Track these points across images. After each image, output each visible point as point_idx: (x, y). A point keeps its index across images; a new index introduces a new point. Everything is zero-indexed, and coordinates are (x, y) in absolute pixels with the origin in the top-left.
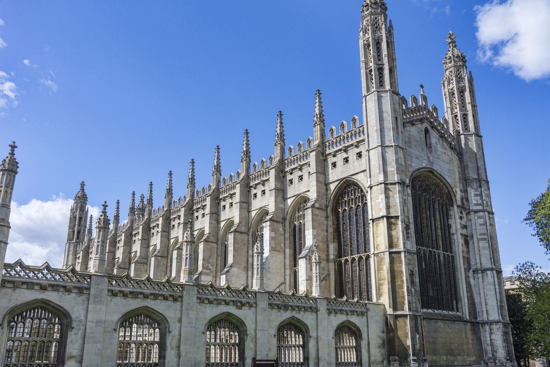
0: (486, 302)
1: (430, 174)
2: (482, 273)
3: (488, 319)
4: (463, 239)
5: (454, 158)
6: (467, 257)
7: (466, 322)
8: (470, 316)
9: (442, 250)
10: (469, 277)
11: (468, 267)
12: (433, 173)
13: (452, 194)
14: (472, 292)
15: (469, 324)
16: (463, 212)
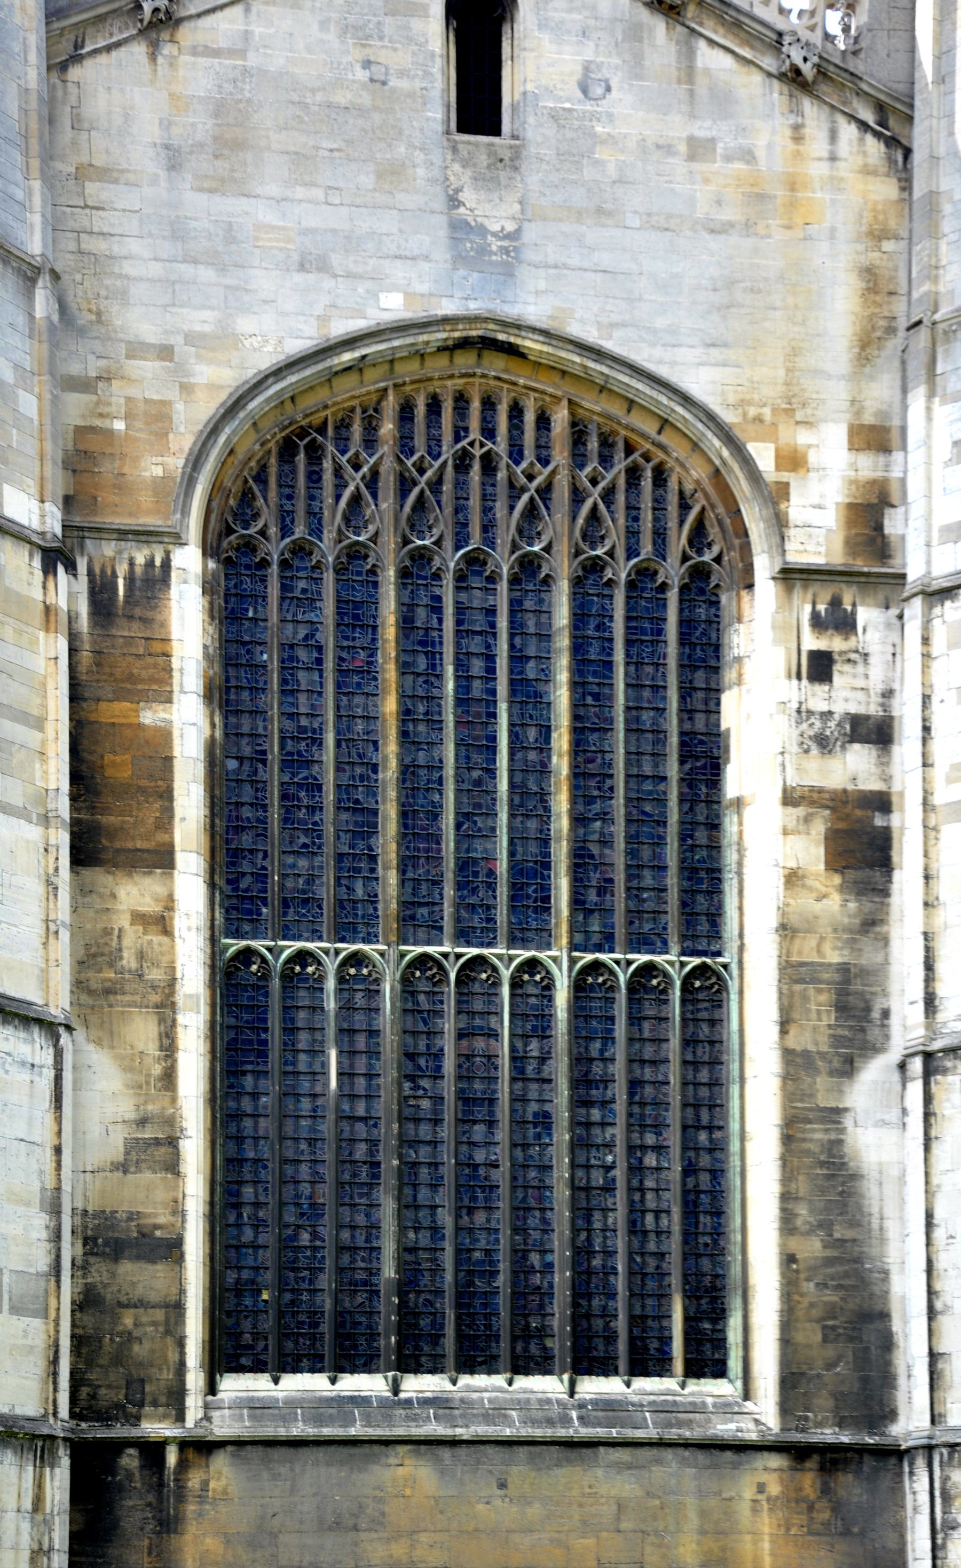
0: (931, 1293)
1: (495, 364)
2: (928, 1074)
3: (935, 1418)
4: (819, 828)
5: (819, 170)
6: (844, 969)
7: (742, 1448)
8: (785, 1409)
9: (564, 941)
10: (834, 1115)
11: (837, 1041)
12: (512, 351)
13: (741, 486)
14: (855, 1224)
15: (775, 1461)
16: (866, 615)
